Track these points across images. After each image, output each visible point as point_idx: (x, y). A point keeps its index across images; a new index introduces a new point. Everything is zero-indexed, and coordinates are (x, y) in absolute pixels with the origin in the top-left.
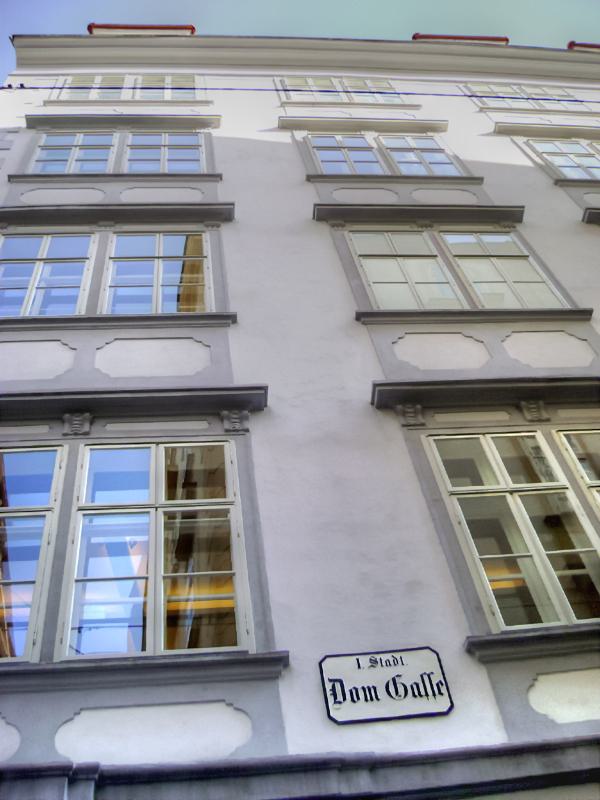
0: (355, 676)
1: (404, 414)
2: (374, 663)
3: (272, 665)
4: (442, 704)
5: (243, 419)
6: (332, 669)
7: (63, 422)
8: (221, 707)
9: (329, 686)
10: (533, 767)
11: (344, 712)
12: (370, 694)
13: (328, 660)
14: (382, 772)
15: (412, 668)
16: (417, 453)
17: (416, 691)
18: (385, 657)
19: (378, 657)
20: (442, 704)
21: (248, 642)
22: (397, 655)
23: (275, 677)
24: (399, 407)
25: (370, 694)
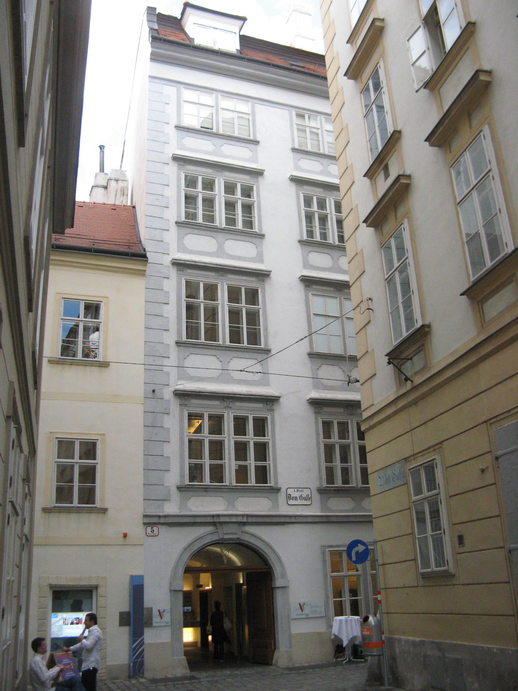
0: (294, 494)
1: (315, 407)
2: (297, 490)
3: (277, 490)
4: (309, 502)
5: (273, 405)
6: (290, 491)
7: (224, 401)
8: (267, 499)
9: (288, 495)
10: (325, 520)
11: (291, 502)
12: (296, 498)
13: (288, 489)
14: (297, 518)
15: (306, 493)
16: (317, 422)
17: (305, 499)
18: (300, 489)
19: (298, 489)
20: (309, 502)
21: (271, 483)
22: (303, 489)
23: (277, 493)
24: (315, 405)
25: (296, 498)
